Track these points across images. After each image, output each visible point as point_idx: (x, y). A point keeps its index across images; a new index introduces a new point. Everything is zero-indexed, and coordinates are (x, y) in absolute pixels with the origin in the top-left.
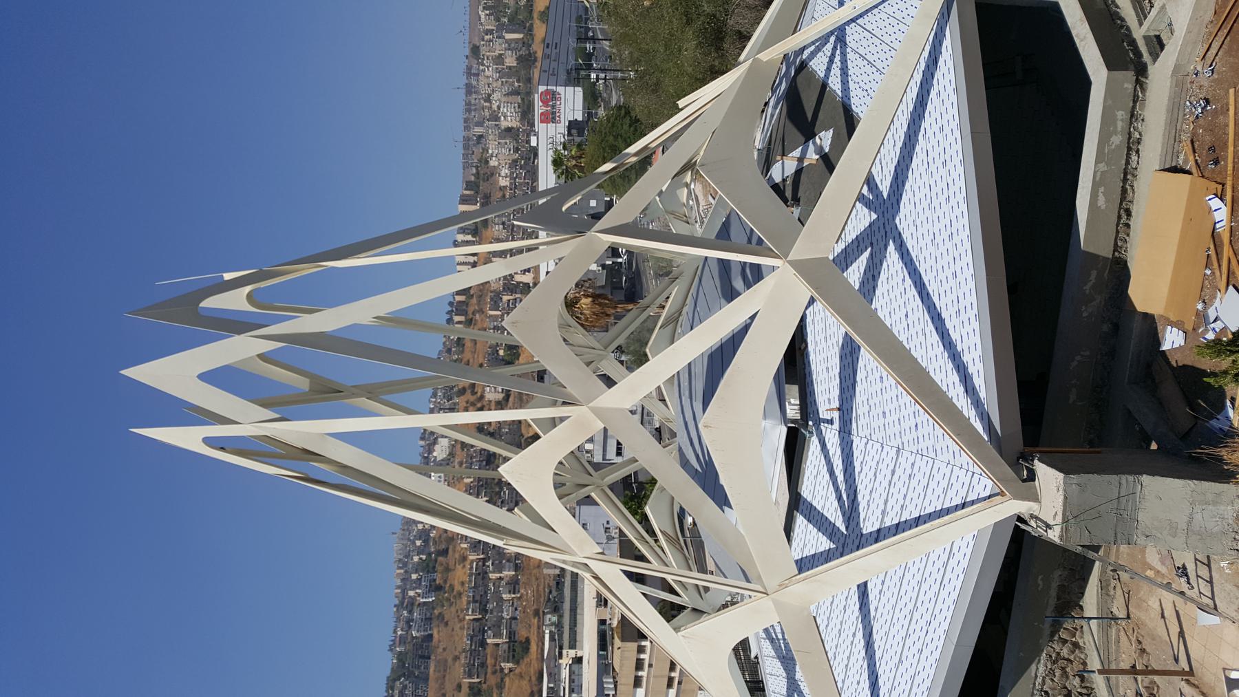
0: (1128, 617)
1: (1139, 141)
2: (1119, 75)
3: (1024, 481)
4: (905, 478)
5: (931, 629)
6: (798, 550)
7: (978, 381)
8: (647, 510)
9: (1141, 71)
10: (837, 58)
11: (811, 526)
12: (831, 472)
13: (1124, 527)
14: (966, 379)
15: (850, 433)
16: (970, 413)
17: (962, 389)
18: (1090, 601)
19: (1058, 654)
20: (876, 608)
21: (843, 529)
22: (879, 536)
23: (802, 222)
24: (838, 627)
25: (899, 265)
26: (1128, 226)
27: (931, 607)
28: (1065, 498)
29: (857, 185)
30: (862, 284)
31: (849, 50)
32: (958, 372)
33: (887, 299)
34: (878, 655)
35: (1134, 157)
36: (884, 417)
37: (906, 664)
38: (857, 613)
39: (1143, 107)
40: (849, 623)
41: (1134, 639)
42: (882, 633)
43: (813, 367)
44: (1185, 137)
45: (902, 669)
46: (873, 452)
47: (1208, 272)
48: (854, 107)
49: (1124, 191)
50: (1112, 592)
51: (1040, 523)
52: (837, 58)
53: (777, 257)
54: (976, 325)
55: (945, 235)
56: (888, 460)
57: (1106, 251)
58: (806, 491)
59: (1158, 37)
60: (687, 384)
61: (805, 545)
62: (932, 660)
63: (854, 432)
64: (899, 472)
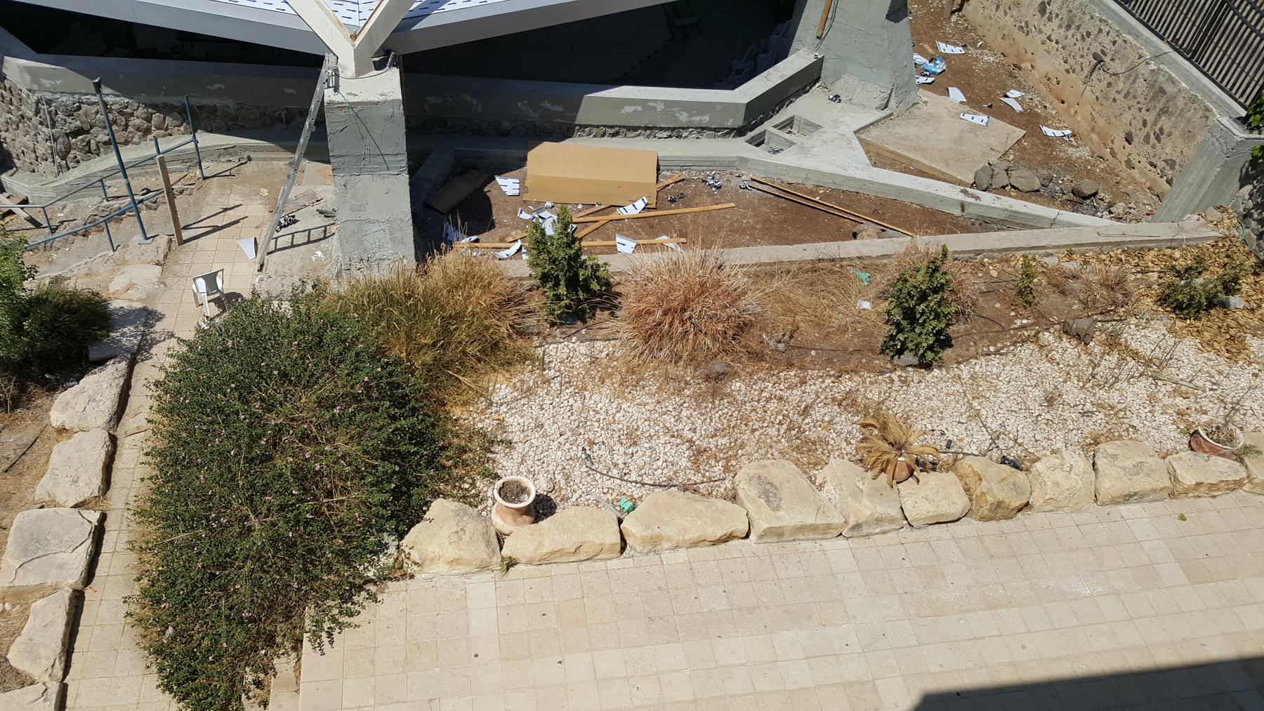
0: (205, 178)
1: (679, 137)
9: (740, 132)
13: (358, 164)
18: (207, 140)
19: (132, 115)
26: (603, 136)
28: (377, 103)
35: (665, 134)
39: (709, 137)
44: (685, 175)
47: (580, 207)
49: (635, 129)
57: (581, 118)
59: (762, 142)
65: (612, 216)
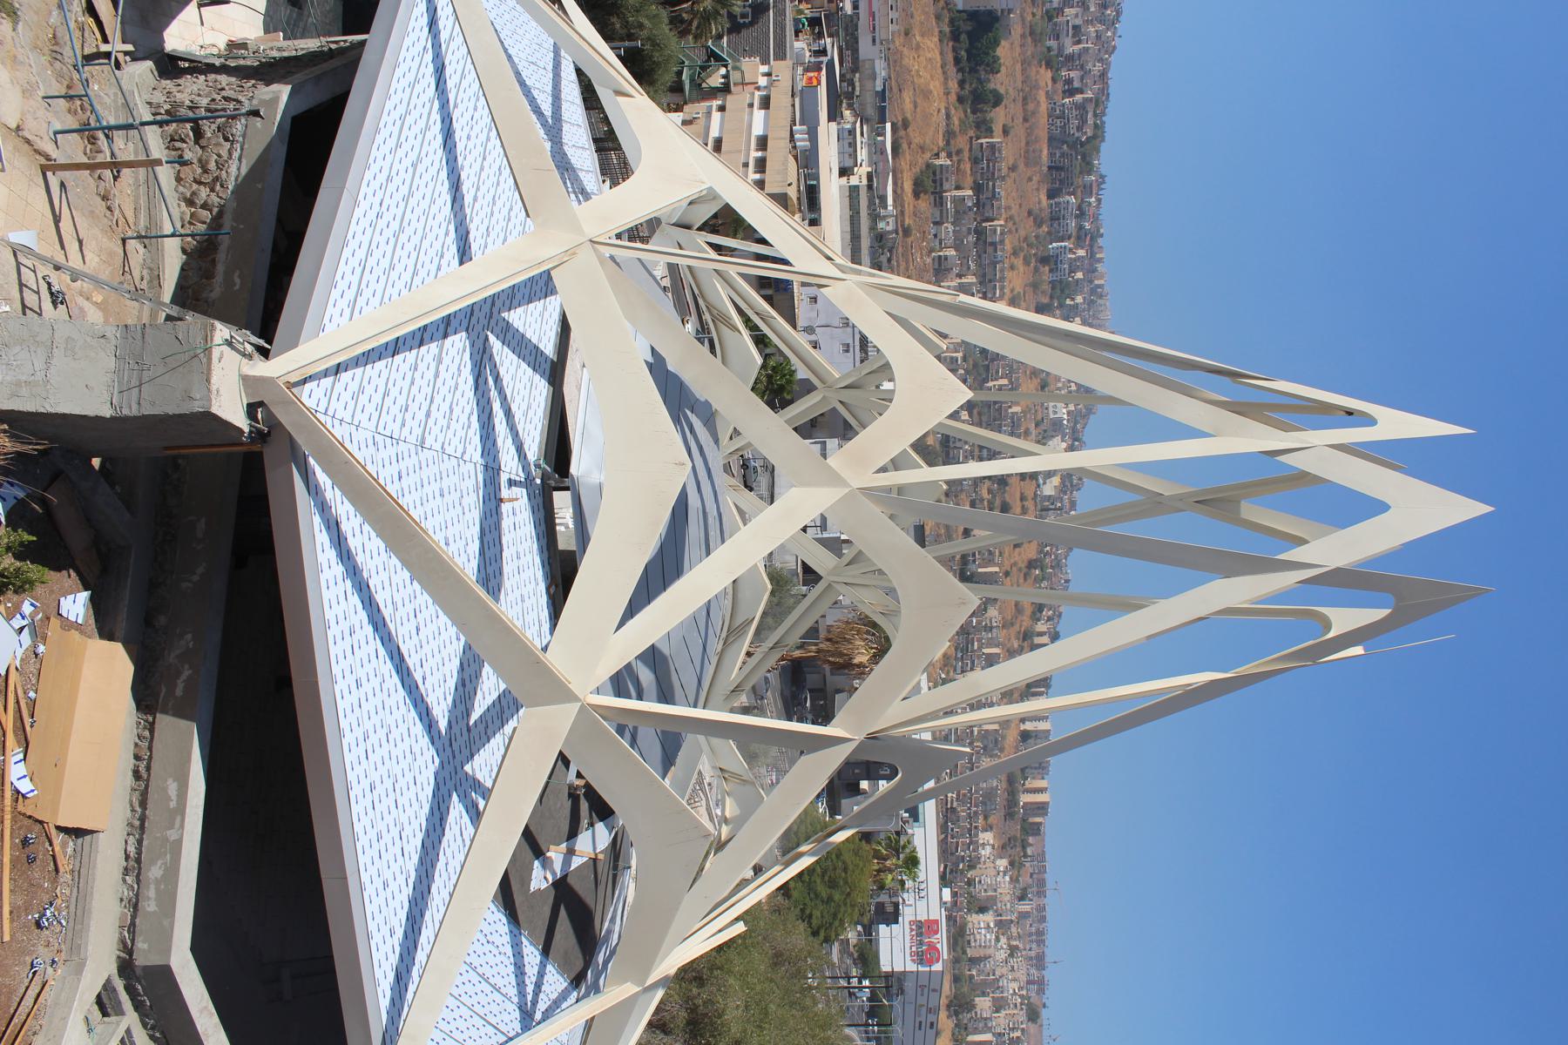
0: (124, 241)
1: (126, 871)
2: (155, 960)
3: (261, 404)
4: (413, 407)
5: (376, 208)
6: (550, 308)
7: (322, 538)
8: (759, 361)
9: (126, 967)
10: (530, 989)
11: (534, 341)
12: (508, 413)
13: (133, 346)
14: (339, 541)
15: (486, 467)
16: (332, 494)
17: (344, 527)
19: (212, 190)
20: (447, 234)
21: (492, 338)
22: (446, 327)
23: (563, 759)
24: (496, 209)
25: (431, 700)
26: (137, 757)
27: (377, 238)
28: (208, 380)
29: (492, 810)
30: (478, 675)
31: (516, 1000)
32: (349, 551)
33: (445, 653)
34: (444, 174)
35: (132, 850)
36: (441, 490)
37: (407, 162)
38: (472, 227)
39: (123, 915)
40: (482, 214)
41: (117, 212)
42: (440, 202)
43: (538, 560)
44: (65, 877)
45: (413, 156)
46: (455, 441)
47: (32, 694)
48: (504, 920)
49: (143, 803)
50: (145, 272)
51: (240, 347)
52: (530, 989)
53: (596, 708)
54: (330, 615)
55: (373, 739)
56: (436, 430)
57: (164, 721)
58: (542, 388)
60: (712, 533)
61: (542, 315)
62: (374, 168)
63: (480, 469)
64: (421, 415)
65: (11, 740)
